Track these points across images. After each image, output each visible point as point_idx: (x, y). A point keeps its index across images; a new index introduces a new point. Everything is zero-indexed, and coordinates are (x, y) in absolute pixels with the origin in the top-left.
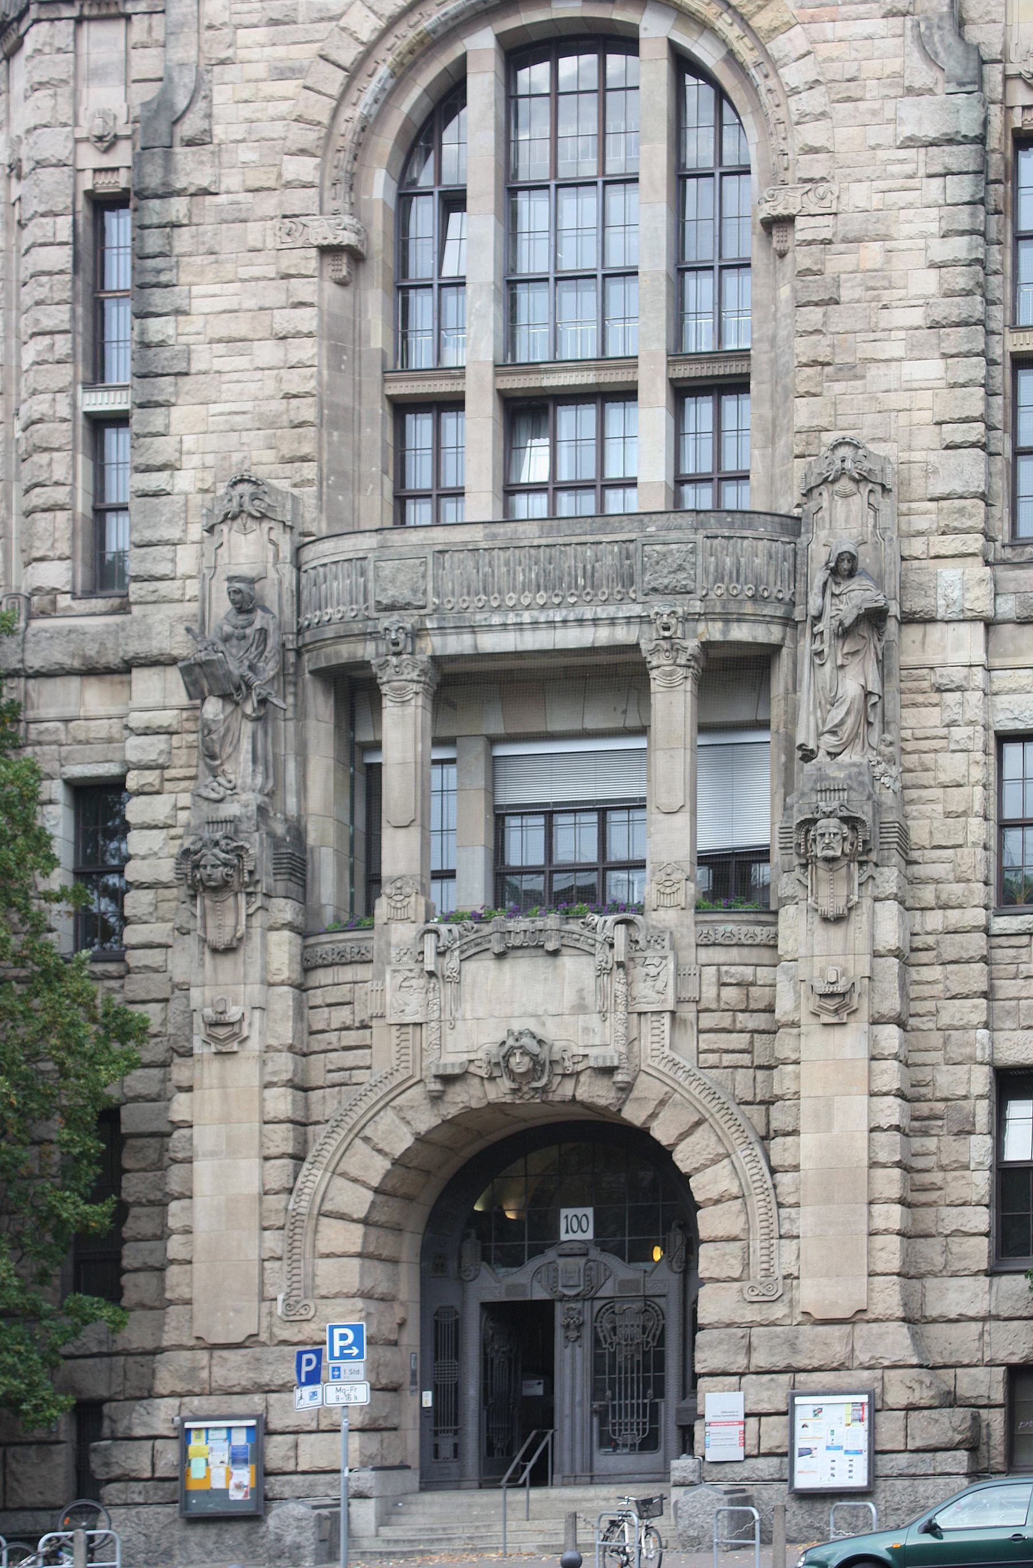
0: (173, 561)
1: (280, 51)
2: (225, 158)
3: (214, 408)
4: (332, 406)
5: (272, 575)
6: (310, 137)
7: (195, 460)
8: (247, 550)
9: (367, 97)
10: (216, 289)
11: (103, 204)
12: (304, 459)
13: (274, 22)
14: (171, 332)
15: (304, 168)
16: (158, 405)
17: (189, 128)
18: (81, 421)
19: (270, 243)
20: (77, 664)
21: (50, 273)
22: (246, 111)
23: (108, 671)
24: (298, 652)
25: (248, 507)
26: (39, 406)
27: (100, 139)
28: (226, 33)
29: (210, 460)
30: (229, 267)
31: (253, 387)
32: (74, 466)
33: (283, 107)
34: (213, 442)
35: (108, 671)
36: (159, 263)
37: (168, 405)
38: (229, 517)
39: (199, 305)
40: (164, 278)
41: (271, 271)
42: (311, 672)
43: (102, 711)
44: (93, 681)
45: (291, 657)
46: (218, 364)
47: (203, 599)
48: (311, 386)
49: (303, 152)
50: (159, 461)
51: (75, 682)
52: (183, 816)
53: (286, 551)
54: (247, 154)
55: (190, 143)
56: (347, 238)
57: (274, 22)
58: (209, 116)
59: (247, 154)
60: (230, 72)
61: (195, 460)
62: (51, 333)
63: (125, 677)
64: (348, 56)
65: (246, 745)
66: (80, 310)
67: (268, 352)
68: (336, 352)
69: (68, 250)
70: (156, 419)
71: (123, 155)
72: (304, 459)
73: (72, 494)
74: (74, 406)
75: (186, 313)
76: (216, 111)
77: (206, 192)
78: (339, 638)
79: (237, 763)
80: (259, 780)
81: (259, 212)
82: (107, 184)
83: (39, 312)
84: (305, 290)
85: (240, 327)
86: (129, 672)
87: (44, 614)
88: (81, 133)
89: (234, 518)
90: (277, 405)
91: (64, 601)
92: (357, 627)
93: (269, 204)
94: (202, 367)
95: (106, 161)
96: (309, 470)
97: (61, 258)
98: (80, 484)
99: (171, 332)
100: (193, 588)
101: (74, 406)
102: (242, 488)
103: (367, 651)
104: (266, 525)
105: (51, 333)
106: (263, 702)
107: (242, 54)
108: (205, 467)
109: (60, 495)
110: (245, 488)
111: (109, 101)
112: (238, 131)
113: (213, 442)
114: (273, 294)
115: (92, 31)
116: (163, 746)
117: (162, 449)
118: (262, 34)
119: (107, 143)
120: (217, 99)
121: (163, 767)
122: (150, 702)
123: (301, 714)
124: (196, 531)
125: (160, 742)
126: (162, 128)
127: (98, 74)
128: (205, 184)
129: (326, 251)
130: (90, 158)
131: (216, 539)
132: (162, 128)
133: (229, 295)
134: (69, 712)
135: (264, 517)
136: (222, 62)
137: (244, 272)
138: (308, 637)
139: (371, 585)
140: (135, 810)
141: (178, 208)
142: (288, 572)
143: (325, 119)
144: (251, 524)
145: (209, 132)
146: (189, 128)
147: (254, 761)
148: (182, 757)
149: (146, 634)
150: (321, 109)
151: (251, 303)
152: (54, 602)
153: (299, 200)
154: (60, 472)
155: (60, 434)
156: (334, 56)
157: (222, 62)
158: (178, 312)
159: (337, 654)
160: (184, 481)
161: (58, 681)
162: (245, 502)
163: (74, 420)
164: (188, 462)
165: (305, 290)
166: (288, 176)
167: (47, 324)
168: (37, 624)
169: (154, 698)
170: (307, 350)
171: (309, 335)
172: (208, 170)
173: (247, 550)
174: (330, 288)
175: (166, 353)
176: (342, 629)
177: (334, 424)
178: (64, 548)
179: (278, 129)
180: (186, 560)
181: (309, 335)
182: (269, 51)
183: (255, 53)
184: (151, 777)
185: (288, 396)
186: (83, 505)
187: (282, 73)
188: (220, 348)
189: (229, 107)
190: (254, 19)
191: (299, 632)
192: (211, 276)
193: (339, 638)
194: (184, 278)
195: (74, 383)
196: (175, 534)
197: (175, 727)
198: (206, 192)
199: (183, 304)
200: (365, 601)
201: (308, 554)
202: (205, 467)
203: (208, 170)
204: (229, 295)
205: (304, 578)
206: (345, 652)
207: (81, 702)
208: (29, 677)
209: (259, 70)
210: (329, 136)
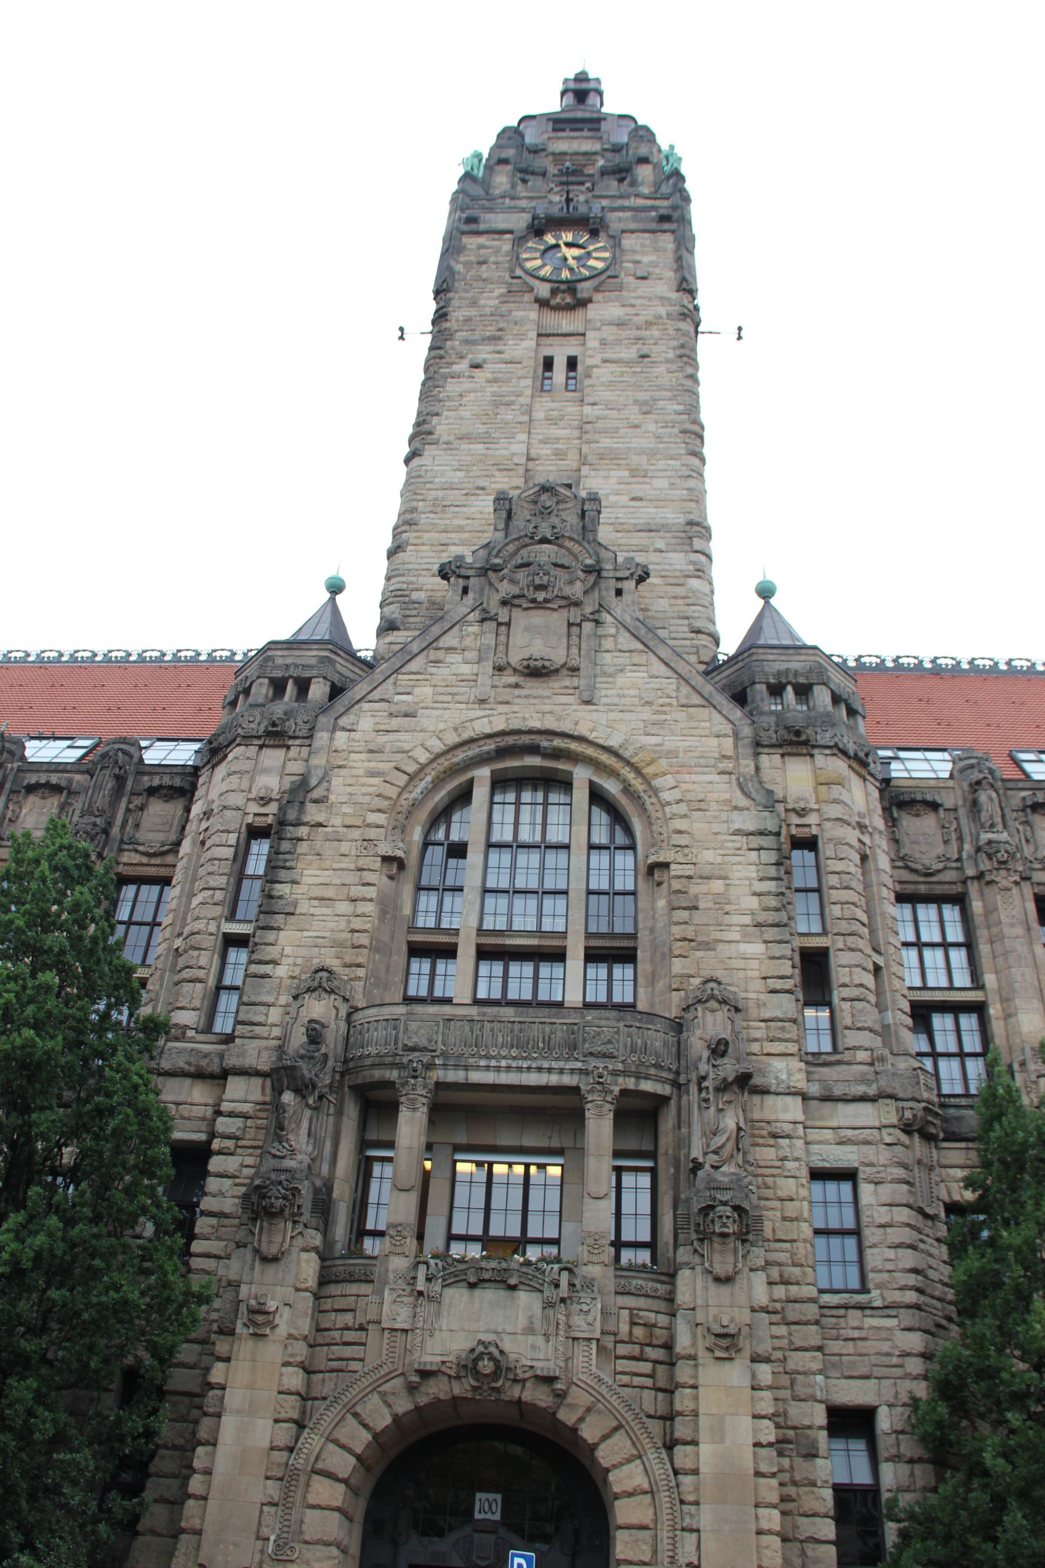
0: (267, 1015)
1: (373, 765)
2: (334, 811)
3: (306, 934)
4: (378, 941)
5: (333, 1026)
6: (384, 804)
7: (290, 960)
8: (318, 1008)
9: (418, 790)
10: (318, 872)
11: (255, 833)
12: (359, 966)
13: (371, 751)
14: (288, 891)
15: (380, 818)
16: (272, 928)
17: (315, 794)
18: (220, 937)
19: (353, 853)
20: (192, 1069)
21: (220, 860)
22: (349, 789)
23: (212, 1076)
24: (342, 1074)
25: (324, 984)
26: (200, 925)
27: (262, 798)
28: (344, 755)
29: (299, 961)
30: (328, 862)
31: (332, 925)
32: (212, 960)
33: (371, 790)
34: (303, 951)
35: (212, 1076)
36: (288, 857)
37: (279, 929)
38: (310, 990)
39: (305, 880)
40: (288, 864)
41: (352, 866)
42: (350, 1087)
43: (202, 1101)
44: (199, 1082)
45: (338, 1077)
46: (312, 911)
47: (284, 1039)
48: (368, 926)
49: (379, 811)
50: (268, 958)
51: (188, 1081)
52: (247, 1172)
53: (343, 1013)
54: (346, 809)
55: (316, 801)
56: (400, 853)
57: (371, 751)
58: (328, 790)
59: (346, 809)
60: (343, 772)
61: (290, 960)
62: (214, 889)
63: (222, 1082)
64: (411, 768)
65: (305, 1124)
66: (232, 880)
67: (344, 907)
68: (383, 913)
69: (232, 850)
70: (271, 936)
71: (273, 808)
72: (359, 966)
73: (208, 975)
74: (218, 927)
75: (298, 883)
76: (332, 788)
77: (321, 825)
78: (374, 1066)
79: (298, 1135)
80: (310, 1148)
81: (349, 837)
82: (260, 822)
83: (209, 878)
84: (369, 877)
85: (330, 893)
86: (226, 1079)
87: (176, 1039)
88: (251, 796)
89: (314, 990)
90: (346, 935)
91: (190, 1033)
92: (388, 1060)
93: (356, 834)
94: (303, 911)
95: (262, 810)
96: (361, 972)
97: (229, 852)
98: (213, 970)
99: (288, 891)
100: (276, 1032)
101: (218, 927)
102: (321, 974)
103: (393, 1075)
104: (333, 997)
105: (214, 889)
106: (321, 1097)
107: (351, 764)
108: (295, 965)
109: (201, 974)
110: (324, 974)
111: (271, 783)
112: (344, 799)
113: (303, 951)
114: (351, 878)
115: (267, 752)
116: (241, 1125)
117: (271, 952)
118: (363, 756)
119: (264, 801)
120: (333, 783)
121: (237, 1138)
122: (236, 1097)
123: (340, 1113)
124: (284, 999)
125: (239, 1122)
126: (300, 792)
127: (266, 771)
128: (321, 820)
129: (386, 859)
130: (253, 808)
131: (299, 1002)
132: (300, 792)
133: (325, 877)
134: (180, 1099)
135: (332, 992)
136: (340, 767)
137: (335, 866)
138: (351, 1065)
139: (401, 1035)
140: (215, 1164)
141: (303, 831)
142: (343, 1025)
143: (394, 797)
144: (324, 995)
145: (327, 797)
146: (315, 794)
147: (309, 1135)
148: (251, 1133)
149: (243, 1054)
150: (393, 792)
151: (338, 882)
152: (184, 1034)
153: (372, 833)
154: (203, 962)
155: (208, 942)
156: (404, 768)
157: (340, 767)
158: (294, 882)
159: (371, 1076)
160: (281, 971)
161: (178, 1079)
162: (320, 981)
163: (216, 935)
164: (284, 961)
165: (369, 877)
166: (369, 821)
167: (212, 884)
168: (170, 1044)
169: (240, 1094)
170: (369, 908)
171: (371, 900)
172: (323, 814)
173: (318, 1008)
174: (385, 879)
175: (283, 902)
176: (377, 1060)
177: (377, 950)
178: (197, 1003)
179: (367, 799)
180: (275, 1015)
181: (371, 900)
182: (366, 764)
183: (359, 764)
184: (230, 1144)
185: (353, 931)
186: (211, 982)
187: (372, 774)
188: (315, 903)
189: (339, 787)
190: (361, 749)
191: (346, 1062)
192: (315, 866)
193: (374, 1066)
194: (299, 865)
195: (221, 916)
196: (270, 999)
197: (251, 1113)
198: (321, 825)
199: (297, 878)
200: (396, 1043)
201: (358, 1016)
202: (295, 965)
203: (323, 814)
204: (325, 877)
205: (352, 1031)
206: (377, 1074)
207: (190, 1094)
208: (160, 1074)
209: (361, 772)
210: (395, 805)
